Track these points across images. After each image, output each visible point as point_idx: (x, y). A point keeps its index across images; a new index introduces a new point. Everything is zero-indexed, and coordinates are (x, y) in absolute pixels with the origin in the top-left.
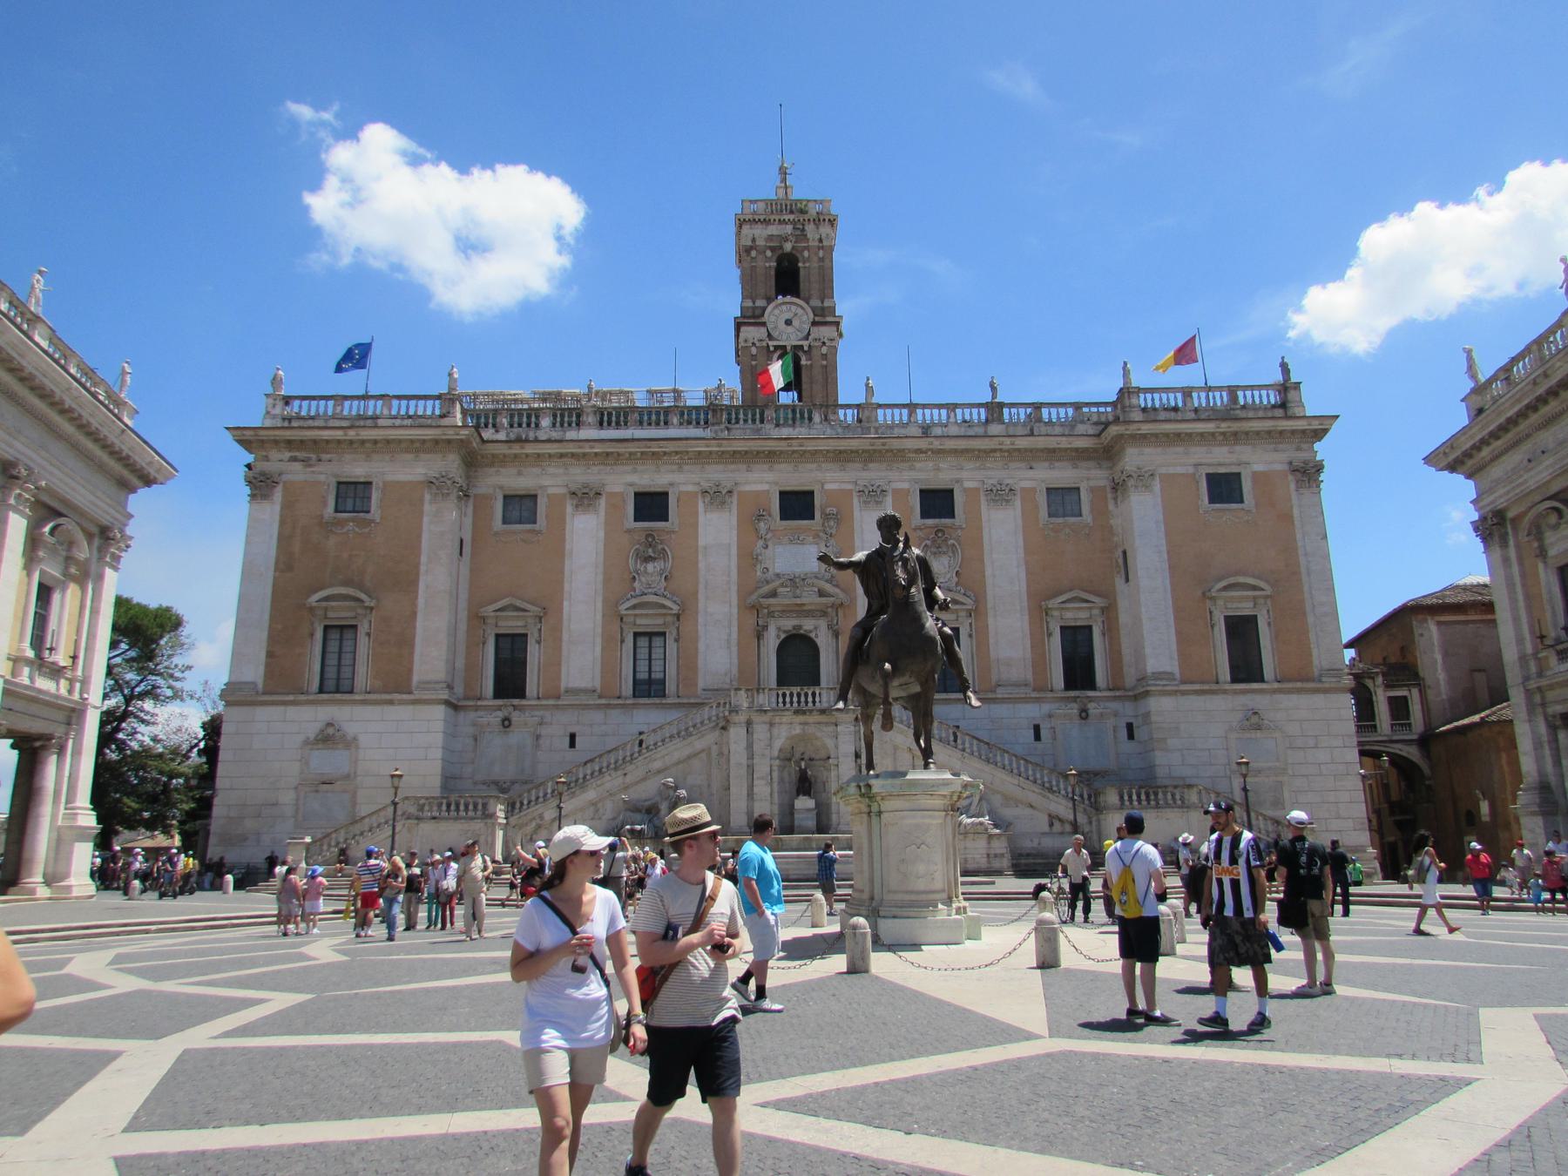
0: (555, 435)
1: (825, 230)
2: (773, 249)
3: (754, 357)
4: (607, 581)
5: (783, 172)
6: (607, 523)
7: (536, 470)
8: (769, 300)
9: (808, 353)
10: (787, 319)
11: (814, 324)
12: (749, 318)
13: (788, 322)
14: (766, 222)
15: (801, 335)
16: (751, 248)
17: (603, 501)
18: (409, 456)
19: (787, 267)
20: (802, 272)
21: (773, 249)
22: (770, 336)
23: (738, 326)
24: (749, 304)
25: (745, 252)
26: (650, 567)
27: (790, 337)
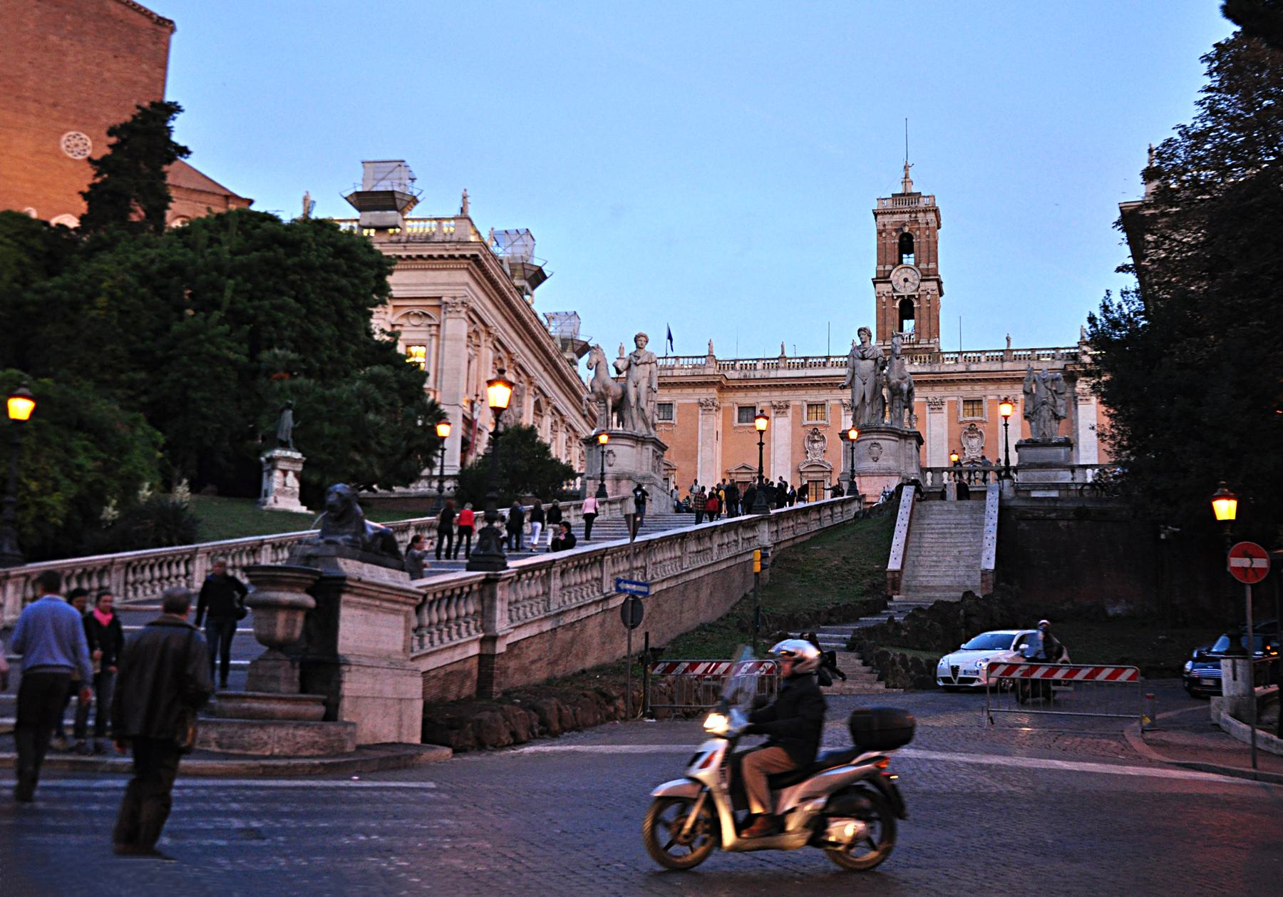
0: (765, 374)
1: (931, 216)
2: (896, 231)
3: (884, 304)
4: (793, 453)
5: (906, 168)
6: (793, 422)
7: (755, 394)
8: (894, 266)
9: (918, 299)
10: (905, 280)
11: (922, 280)
12: (882, 278)
13: (906, 280)
14: (893, 213)
15: (914, 288)
16: (884, 231)
17: (790, 411)
18: (690, 391)
19: (907, 234)
20: (916, 246)
21: (896, 231)
22: (894, 290)
23: (875, 283)
24: (881, 268)
25: (880, 233)
26: (816, 445)
27: (907, 291)
